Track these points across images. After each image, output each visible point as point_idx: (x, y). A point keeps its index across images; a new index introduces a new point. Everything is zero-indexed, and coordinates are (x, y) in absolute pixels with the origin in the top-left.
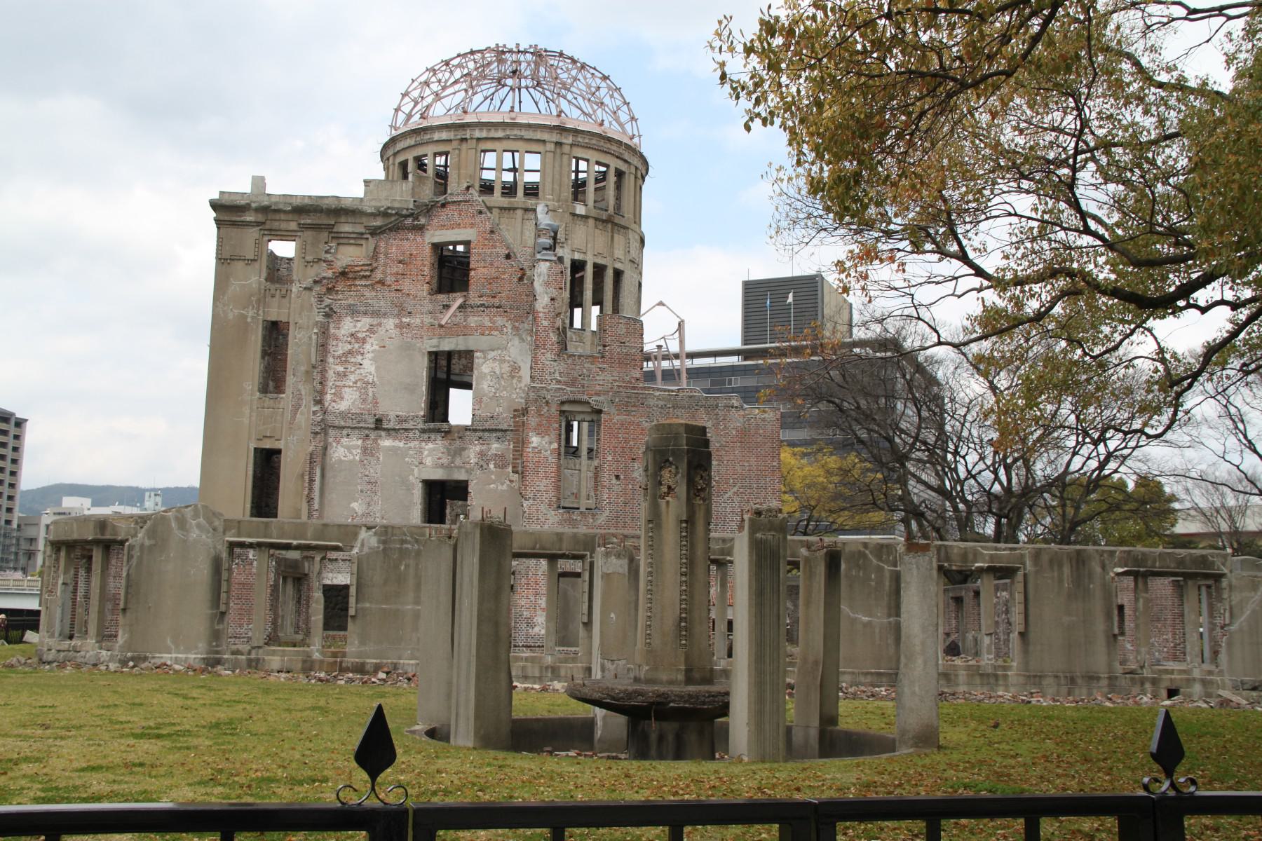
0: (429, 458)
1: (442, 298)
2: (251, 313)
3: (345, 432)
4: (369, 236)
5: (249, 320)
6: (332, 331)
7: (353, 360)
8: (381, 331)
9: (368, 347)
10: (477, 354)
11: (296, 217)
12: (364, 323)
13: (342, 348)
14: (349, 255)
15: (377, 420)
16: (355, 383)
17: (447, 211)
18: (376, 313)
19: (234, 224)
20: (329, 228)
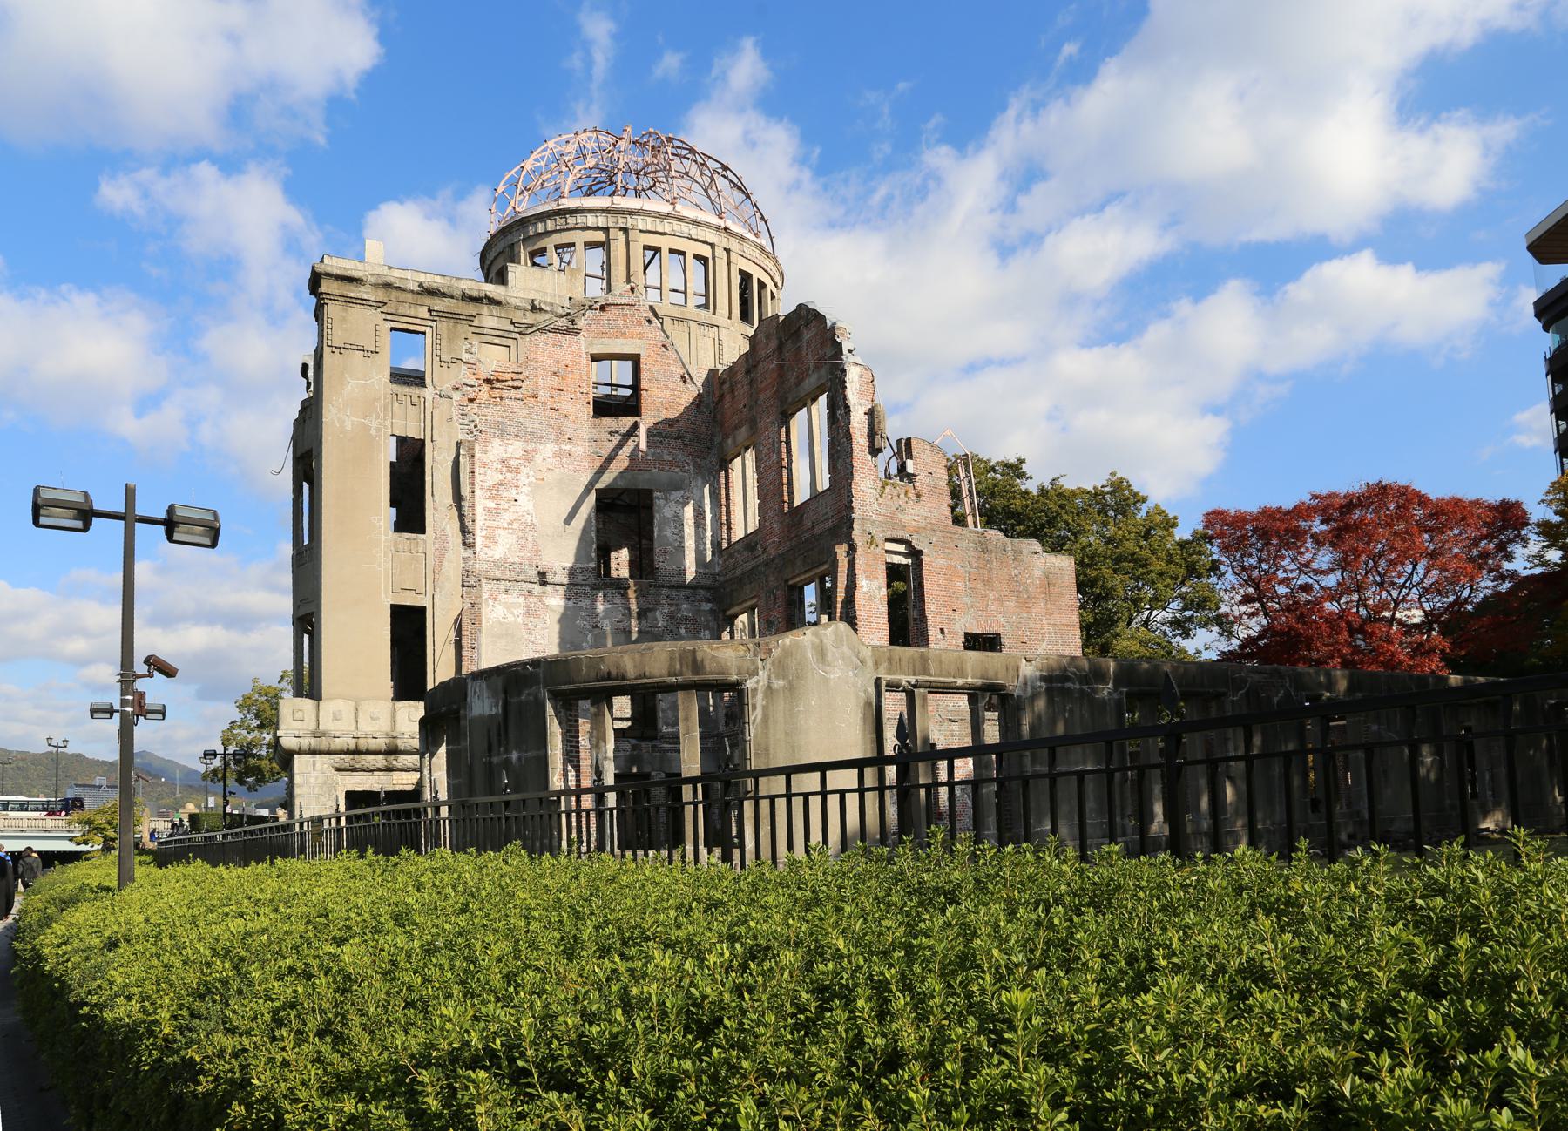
0: (606, 622)
1: (607, 421)
2: (374, 424)
3: (503, 585)
4: (518, 336)
5: (373, 432)
6: (478, 455)
7: (505, 494)
8: (538, 459)
9: (522, 479)
10: (657, 494)
11: (428, 301)
12: (516, 448)
13: (493, 478)
14: (493, 359)
15: (539, 573)
16: (511, 524)
17: (607, 315)
18: (530, 436)
19: (346, 300)
20: (470, 318)
